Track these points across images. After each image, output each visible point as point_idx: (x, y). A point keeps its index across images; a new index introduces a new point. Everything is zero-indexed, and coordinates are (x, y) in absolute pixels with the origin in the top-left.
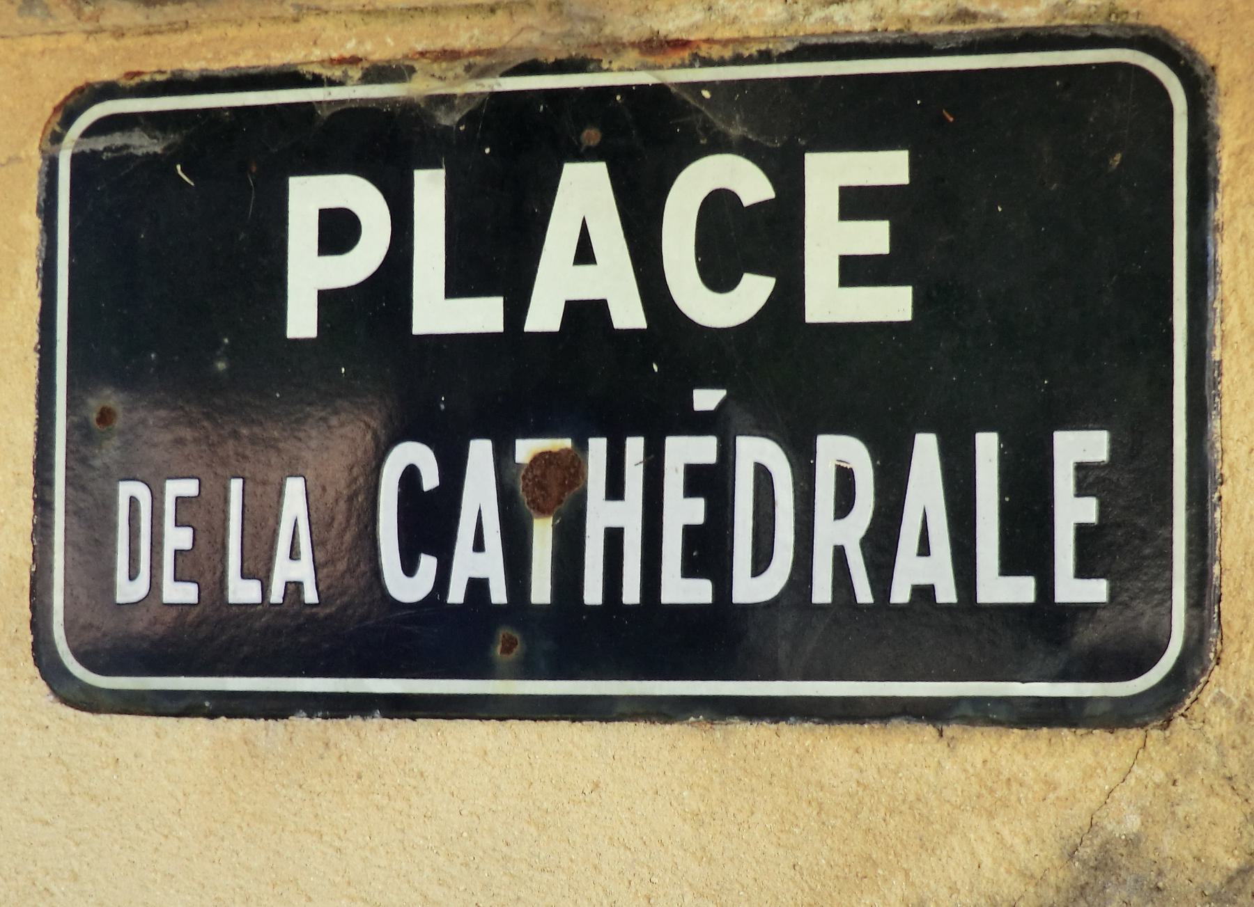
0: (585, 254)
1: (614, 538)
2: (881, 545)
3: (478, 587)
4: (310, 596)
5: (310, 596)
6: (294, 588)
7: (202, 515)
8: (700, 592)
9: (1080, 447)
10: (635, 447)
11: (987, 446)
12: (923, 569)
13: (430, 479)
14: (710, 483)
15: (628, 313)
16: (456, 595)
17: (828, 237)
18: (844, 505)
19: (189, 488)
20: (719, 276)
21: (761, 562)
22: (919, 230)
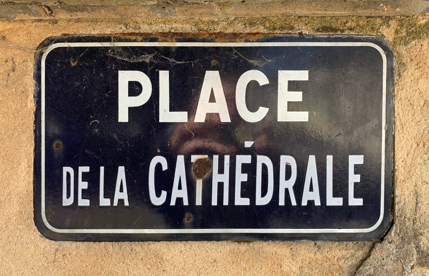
1: (221, 185)
3: (179, 200)
4: (127, 203)
5: (127, 203)
6: (121, 201)
7: (92, 178)
8: (246, 202)
12: (310, 196)
13: (165, 167)
16: (173, 203)
18: (288, 176)
19: (87, 169)
21: (264, 193)
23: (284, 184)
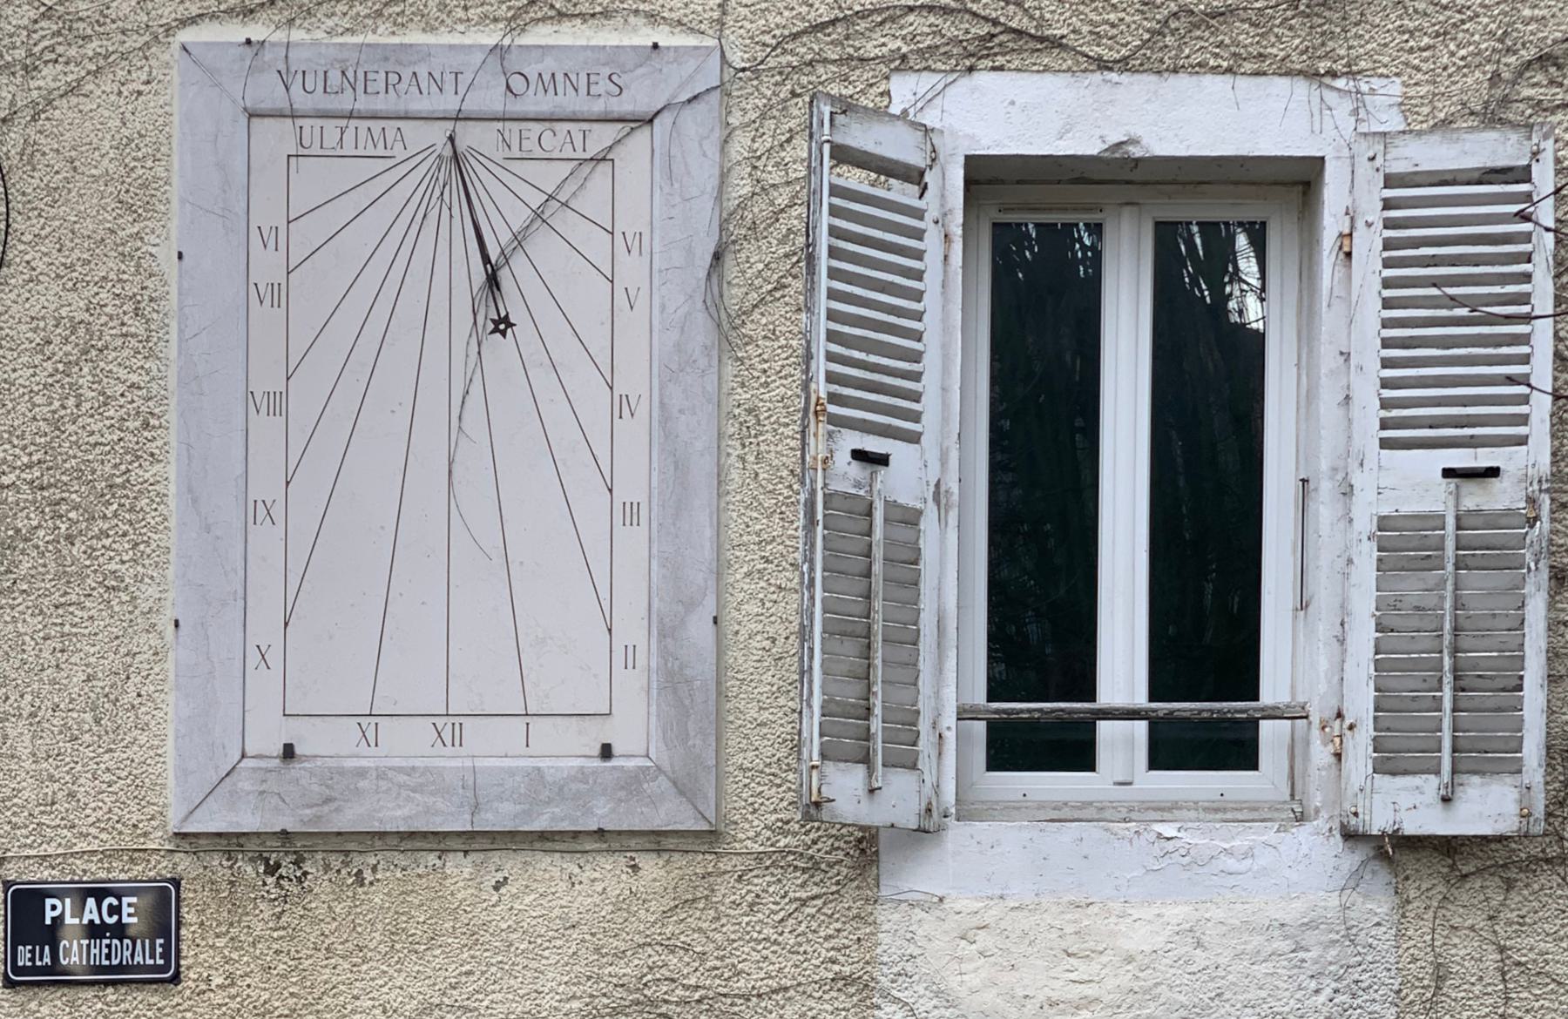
7: (33, 952)
9: (160, 941)
12: (138, 959)
14: (109, 946)
15: (97, 921)
17: (126, 910)
20: (110, 915)
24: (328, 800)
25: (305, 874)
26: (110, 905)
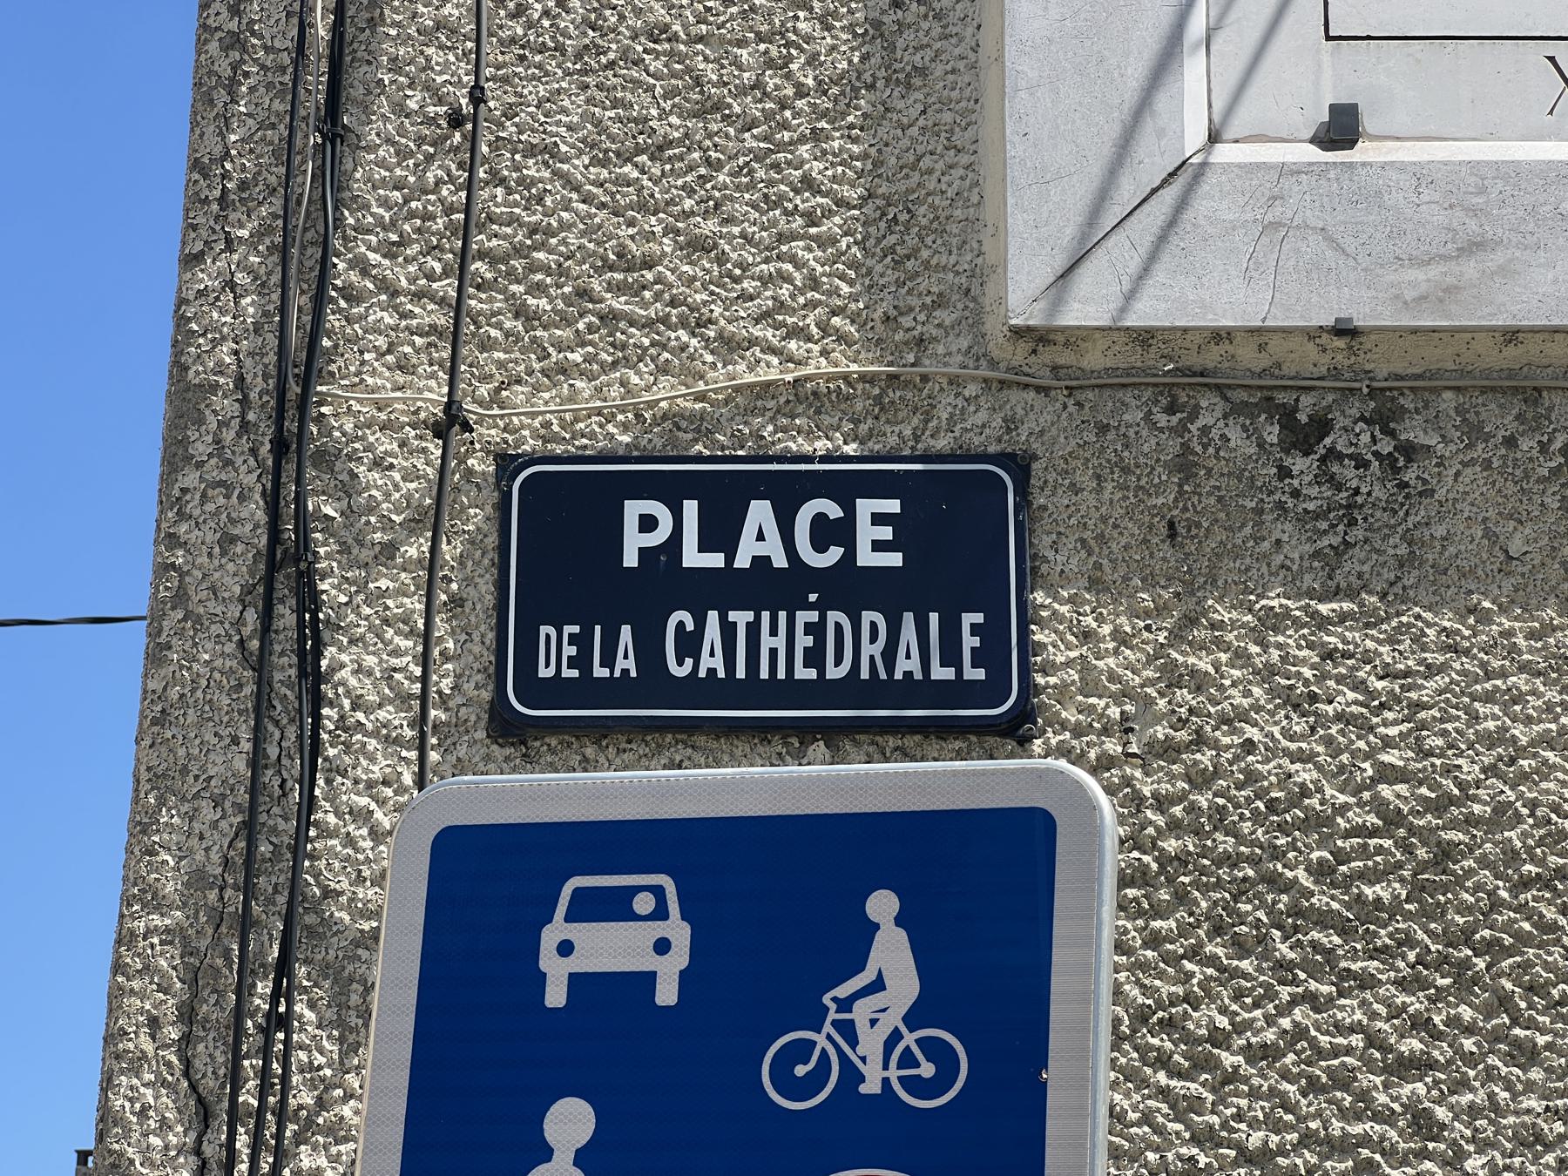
0: (761, 537)
1: (773, 652)
2: (890, 655)
4: (633, 674)
5: (633, 674)
6: (625, 672)
7: (582, 642)
8: (812, 674)
9: (970, 619)
10: (782, 615)
11: (934, 618)
13: (690, 627)
14: (816, 630)
15: (780, 561)
16: (702, 674)
17: (866, 533)
18: (873, 639)
19: (576, 629)
20: (819, 546)
21: (838, 661)
22: (905, 532)
23: (867, 649)
24: (1474, 247)
25: (1409, 451)
26: (819, 520)
